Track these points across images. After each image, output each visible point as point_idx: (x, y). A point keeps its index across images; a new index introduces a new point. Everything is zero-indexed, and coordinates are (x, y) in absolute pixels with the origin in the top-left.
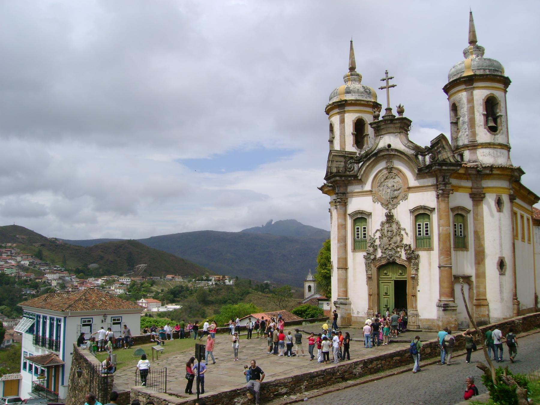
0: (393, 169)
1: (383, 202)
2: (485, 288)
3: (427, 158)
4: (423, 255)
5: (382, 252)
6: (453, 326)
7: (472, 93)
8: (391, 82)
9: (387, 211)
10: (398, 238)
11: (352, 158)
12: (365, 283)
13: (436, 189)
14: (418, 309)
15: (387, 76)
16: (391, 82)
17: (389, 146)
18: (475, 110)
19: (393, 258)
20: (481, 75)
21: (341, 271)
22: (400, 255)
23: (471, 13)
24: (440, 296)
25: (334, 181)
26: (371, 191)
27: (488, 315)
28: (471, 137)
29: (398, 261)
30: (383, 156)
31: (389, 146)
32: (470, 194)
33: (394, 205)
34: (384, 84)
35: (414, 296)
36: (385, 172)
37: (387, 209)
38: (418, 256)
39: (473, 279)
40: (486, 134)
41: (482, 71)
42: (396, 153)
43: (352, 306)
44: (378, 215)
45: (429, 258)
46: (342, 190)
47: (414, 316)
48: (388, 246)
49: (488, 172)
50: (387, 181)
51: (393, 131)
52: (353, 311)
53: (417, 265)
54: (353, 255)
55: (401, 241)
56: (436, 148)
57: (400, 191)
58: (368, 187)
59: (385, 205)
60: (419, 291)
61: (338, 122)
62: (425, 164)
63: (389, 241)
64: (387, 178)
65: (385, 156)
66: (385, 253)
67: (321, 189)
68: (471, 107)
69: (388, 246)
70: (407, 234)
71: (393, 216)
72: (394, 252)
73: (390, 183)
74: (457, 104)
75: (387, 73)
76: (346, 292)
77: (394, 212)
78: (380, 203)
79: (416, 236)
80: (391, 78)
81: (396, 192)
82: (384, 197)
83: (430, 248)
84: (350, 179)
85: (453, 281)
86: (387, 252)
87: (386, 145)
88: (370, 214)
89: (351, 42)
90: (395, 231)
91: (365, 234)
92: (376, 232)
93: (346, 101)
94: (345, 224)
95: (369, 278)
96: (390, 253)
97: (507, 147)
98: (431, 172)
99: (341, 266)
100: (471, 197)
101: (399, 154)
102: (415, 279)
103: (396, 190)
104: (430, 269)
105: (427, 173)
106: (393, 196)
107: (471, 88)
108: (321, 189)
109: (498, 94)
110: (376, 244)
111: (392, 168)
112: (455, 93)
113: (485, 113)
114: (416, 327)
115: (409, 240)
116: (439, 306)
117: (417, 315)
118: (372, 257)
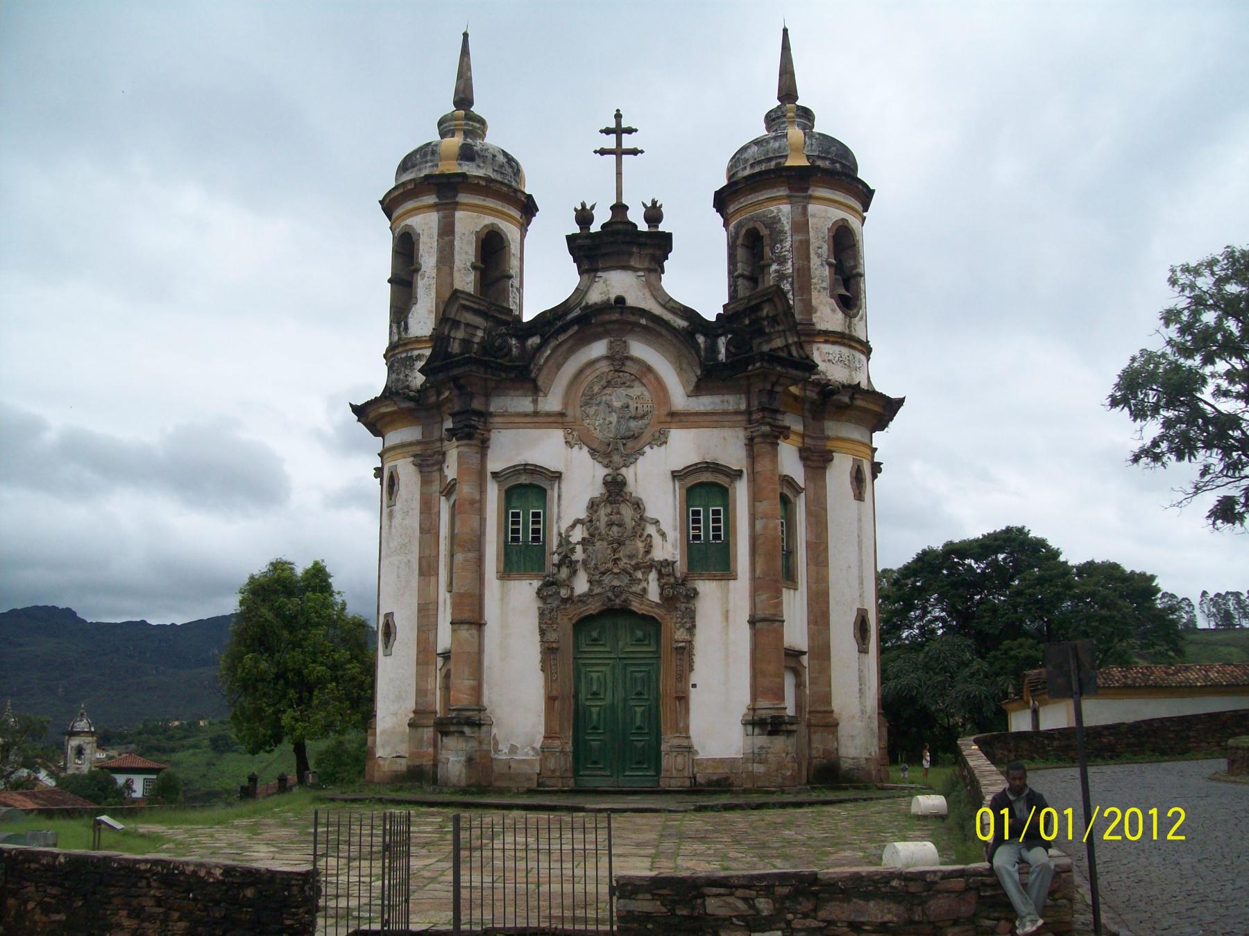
0: (629, 363)
3: (722, 342)
4: (707, 589)
5: (590, 581)
6: (789, 773)
7: (805, 209)
8: (628, 142)
9: (607, 471)
10: (640, 545)
11: (506, 323)
12: (539, 666)
13: (744, 424)
14: (693, 732)
15: (618, 123)
16: (628, 142)
17: (620, 300)
18: (812, 251)
19: (623, 597)
20: (825, 171)
21: (465, 633)
22: (644, 590)
24: (754, 697)
26: (562, 414)
28: (801, 313)
29: (636, 606)
31: (620, 300)
32: (801, 450)
34: (610, 142)
35: (683, 699)
36: (604, 367)
37: (606, 466)
38: (696, 593)
39: (805, 660)
40: (833, 311)
41: (827, 163)
42: (643, 321)
43: (495, 731)
44: (581, 480)
45: (726, 600)
46: (476, 404)
47: (679, 753)
48: (610, 565)
49: (846, 399)
50: (608, 391)
52: (496, 743)
53: (691, 615)
54: (503, 586)
55: (648, 552)
56: (747, 322)
57: (645, 421)
58: (552, 402)
59: (602, 453)
60: (694, 686)
61: (435, 231)
62: (716, 359)
63: (614, 551)
64: (609, 384)
65: (609, 327)
66: (600, 582)
67: (356, 410)
68: (801, 241)
69: (610, 565)
70: (663, 535)
71: (623, 483)
72: (626, 580)
73: (617, 398)
74: (764, 232)
75: (618, 116)
76: (478, 690)
77: (628, 473)
78: (585, 449)
79: (688, 541)
80: (630, 131)
81: (633, 424)
82: (597, 434)
84: (503, 375)
85: (772, 658)
86: (606, 579)
87: (613, 297)
88: (557, 476)
89: (466, 35)
90: (630, 524)
91: (536, 531)
92: (573, 526)
93: (464, 175)
95: (549, 652)
96: (616, 583)
97: (866, 349)
99: (467, 615)
100: (802, 458)
101: (651, 324)
102: (685, 653)
103: (635, 418)
107: (804, 197)
108: (356, 410)
109: (854, 222)
110: (574, 557)
112: (760, 203)
113: (833, 261)
114: (687, 783)
115: (669, 548)
117: (689, 749)
118: (564, 593)
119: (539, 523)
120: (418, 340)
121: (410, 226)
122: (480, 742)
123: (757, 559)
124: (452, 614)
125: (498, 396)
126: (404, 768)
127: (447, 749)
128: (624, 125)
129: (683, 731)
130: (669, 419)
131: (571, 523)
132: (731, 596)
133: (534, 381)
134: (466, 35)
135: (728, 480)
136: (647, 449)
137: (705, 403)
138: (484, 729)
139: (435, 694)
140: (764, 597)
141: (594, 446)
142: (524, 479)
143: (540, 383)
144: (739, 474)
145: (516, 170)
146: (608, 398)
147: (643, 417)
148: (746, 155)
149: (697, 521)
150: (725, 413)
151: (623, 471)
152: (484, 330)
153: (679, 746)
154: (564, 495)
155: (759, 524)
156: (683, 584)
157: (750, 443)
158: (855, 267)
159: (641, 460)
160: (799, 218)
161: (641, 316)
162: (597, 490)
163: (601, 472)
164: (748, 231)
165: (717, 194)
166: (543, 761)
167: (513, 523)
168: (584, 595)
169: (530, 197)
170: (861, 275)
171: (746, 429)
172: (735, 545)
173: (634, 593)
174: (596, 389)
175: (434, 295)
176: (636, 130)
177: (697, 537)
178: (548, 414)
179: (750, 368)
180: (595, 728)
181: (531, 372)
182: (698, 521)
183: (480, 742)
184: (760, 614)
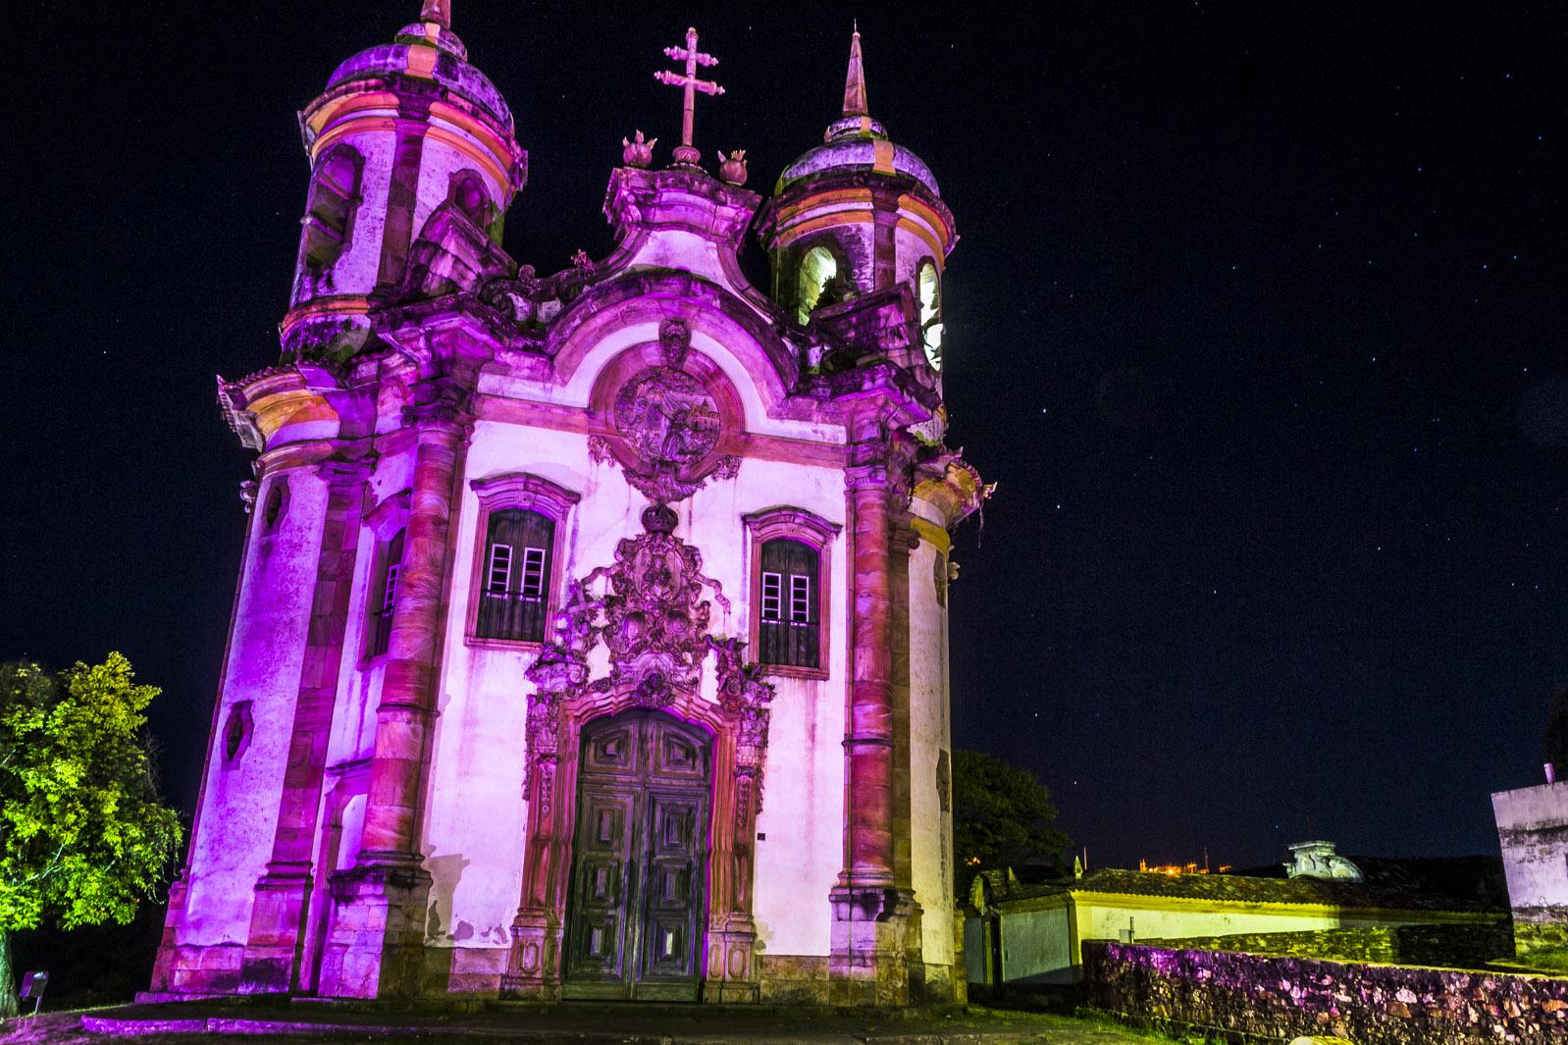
1: (634, 465)
2: (909, 855)
3: (815, 355)
5: (613, 661)
6: (900, 985)
12: (520, 789)
22: (696, 682)
27: (920, 950)
29: (680, 703)
35: (743, 853)
36: (653, 357)
52: (435, 921)
54: (472, 657)
60: (762, 837)
65: (666, 304)
68: (885, 270)
71: (672, 520)
76: (413, 825)
77: (681, 507)
78: (619, 467)
79: (761, 618)
83: (811, 663)
84: (507, 341)
88: (575, 498)
94: (447, 523)
102: (751, 784)
104: (812, 749)
110: (594, 624)
116: (852, 901)
119: (538, 568)
120: (347, 298)
122: (409, 917)
123: (859, 651)
124: (384, 693)
125: (492, 372)
126: (238, 967)
127: (346, 929)
129: (742, 907)
131: (589, 573)
132: (820, 705)
133: (552, 358)
135: (821, 538)
136: (708, 479)
137: (792, 428)
138: (417, 891)
139: (311, 836)
140: (871, 708)
142: (521, 499)
144: (836, 529)
149: (772, 592)
150: (818, 446)
151: (673, 505)
152: (479, 276)
153: (739, 933)
154: (581, 530)
155: (863, 606)
156: (757, 680)
157: (853, 492)
159: (698, 495)
160: (883, 240)
162: (635, 530)
163: (640, 501)
166: (518, 948)
167: (497, 564)
168: (604, 681)
172: (828, 630)
173: (677, 685)
174: (642, 388)
175: (379, 243)
177: (773, 615)
178: (567, 409)
179: (867, 385)
180: (601, 899)
181: (547, 344)
182: (774, 592)
183: (409, 917)
184: (863, 732)
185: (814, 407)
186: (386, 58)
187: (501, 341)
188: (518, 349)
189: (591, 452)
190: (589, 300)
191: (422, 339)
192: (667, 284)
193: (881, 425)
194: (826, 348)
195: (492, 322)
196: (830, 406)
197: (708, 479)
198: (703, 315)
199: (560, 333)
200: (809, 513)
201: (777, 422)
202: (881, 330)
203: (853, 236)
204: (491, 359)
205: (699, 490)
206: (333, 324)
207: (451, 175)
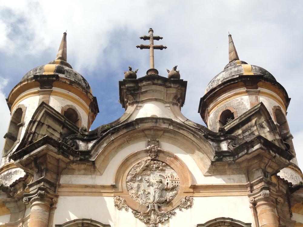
1: (137, 208)
8: (157, 43)
23: (230, 36)
25: (36, 158)
26: (113, 187)
30: (143, 130)
33: (164, 215)
34: (147, 43)
51: (162, 98)
57: (174, 192)
58: (107, 177)
65: (147, 132)
80: (158, 38)
84: (71, 158)
89: (65, 34)
93: (57, 77)
98: (239, 164)
105: (229, 164)
106: (163, 199)
111: (160, 151)
121: (23, 105)
128: (155, 35)
130: (192, 190)
133: (94, 163)
134: (65, 34)
141: (136, 209)
143: (97, 165)
145: (88, 87)
146: (147, 177)
147: (173, 189)
148: (218, 78)
152: (61, 134)
157: (254, 205)
158: (288, 133)
161: (170, 125)
164: (222, 113)
165: (202, 99)
169: (95, 99)
170: (291, 137)
171: (249, 196)
176: (162, 38)
181: (91, 156)
185: (227, 167)
186: (36, 70)
187: (68, 157)
188: (77, 161)
189: (116, 205)
190: (110, 135)
191: (33, 165)
192: (146, 123)
193: (263, 170)
194: (229, 141)
195: (63, 149)
196: (234, 167)
197: (177, 211)
198: (166, 134)
199: (96, 150)
200: (232, 219)
201: (209, 178)
202: (253, 126)
203: (239, 102)
204: (65, 168)
205: (173, 216)
206: (10, 173)
207: (62, 108)
